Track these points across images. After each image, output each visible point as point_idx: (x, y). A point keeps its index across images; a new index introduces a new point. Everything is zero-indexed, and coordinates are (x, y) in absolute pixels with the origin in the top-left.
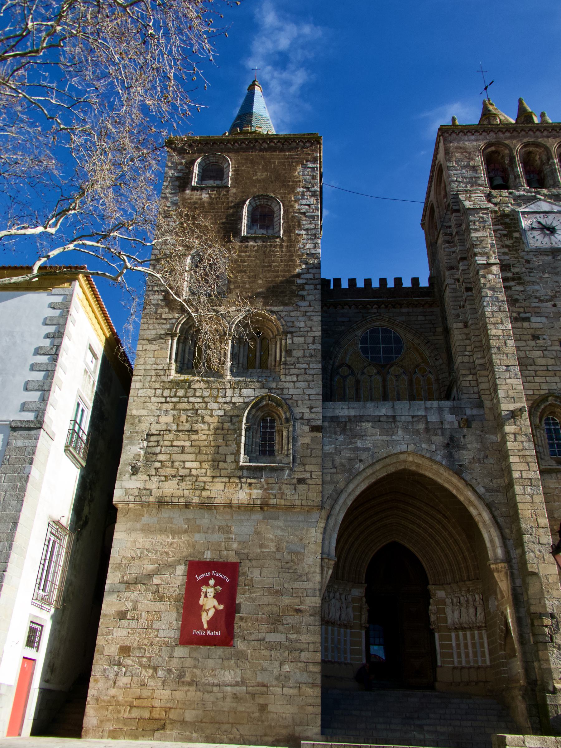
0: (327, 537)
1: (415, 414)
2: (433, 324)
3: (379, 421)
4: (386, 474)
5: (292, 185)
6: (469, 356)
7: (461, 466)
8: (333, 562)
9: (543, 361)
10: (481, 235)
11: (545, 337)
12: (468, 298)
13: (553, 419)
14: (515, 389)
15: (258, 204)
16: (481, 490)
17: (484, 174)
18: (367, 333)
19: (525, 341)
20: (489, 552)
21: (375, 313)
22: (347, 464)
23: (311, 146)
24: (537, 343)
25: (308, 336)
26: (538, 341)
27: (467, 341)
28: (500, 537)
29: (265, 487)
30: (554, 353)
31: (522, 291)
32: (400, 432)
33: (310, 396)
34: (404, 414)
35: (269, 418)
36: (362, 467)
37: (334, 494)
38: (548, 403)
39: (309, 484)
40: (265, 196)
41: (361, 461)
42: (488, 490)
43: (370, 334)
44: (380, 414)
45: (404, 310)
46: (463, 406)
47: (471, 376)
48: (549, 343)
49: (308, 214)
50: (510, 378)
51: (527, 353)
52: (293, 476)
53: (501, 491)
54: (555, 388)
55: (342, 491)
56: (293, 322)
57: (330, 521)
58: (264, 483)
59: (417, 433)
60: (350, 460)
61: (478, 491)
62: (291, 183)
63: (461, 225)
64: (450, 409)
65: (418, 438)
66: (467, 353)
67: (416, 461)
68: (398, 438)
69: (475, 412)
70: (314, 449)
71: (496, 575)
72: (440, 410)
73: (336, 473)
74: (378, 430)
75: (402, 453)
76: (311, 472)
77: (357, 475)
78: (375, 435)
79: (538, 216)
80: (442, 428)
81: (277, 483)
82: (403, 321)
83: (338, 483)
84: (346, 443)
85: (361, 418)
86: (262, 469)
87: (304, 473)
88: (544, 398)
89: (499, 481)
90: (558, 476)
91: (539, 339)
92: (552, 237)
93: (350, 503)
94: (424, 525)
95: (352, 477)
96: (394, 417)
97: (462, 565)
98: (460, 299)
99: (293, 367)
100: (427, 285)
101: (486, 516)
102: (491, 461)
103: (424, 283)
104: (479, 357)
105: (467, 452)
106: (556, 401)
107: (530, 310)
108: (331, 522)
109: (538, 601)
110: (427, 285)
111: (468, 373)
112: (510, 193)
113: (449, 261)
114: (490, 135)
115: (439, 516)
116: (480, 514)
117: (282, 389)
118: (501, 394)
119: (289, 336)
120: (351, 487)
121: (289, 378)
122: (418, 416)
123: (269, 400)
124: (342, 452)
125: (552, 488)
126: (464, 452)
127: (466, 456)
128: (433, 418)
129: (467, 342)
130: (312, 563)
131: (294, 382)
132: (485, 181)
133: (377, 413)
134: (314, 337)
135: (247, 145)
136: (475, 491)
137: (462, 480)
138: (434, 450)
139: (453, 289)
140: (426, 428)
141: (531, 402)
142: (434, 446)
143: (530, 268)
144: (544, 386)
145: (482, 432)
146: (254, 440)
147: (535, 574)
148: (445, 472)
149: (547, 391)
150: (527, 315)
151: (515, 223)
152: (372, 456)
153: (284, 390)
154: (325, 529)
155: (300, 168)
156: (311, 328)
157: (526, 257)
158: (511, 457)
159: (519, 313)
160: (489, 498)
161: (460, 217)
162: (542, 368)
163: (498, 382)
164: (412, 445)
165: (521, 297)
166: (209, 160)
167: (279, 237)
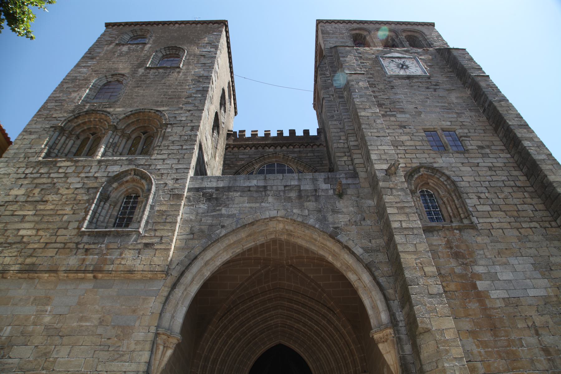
0: (170, 308)
1: (287, 184)
2: (321, 159)
3: (249, 191)
4: (253, 243)
6: (344, 143)
7: (336, 228)
8: (175, 341)
9: (412, 143)
11: (411, 127)
12: (341, 102)
13: (427, 191)
14: (387, 153)
15: (168, 53)
16: (359, 251)
18: (264, 167)
19: (394, 129)
20: (372, 321)
21: (271, 152)
22: (206, 231)
24: (404, 131)
25: (187, 126)
26: (405, 130)
27: (342, 133)
28: (383, 299)
29: (104, 252)
30: (421, 138)
31: (386, 99)
32: (270, 199)
33: (178, 170)
34: (276, 184)
35: (134, 195)
36: (223, 234)
37: (187, 260)
38: (420, 174)
39: (156, 249)
40: (174, 47)
41: (223, 227)
42: (366, 250)
43: (267, 167)
44: (250, 185)
45: (296, 150)
46: (338, 176)
47: (346, 157)
48: (415, 131)
50: (381, 145)
51: (397, 137)
52: (139, 241)
53: (381, 250)
54: (426, 161)
55: (196, 258)
56: (175, 117)
57: (176, 290)
58: (104, 248)
59: (289, 199)
60: (211, 226)
61: (356, 252)
64: (325, 179)
65: (290, 204)
66: (341, 141)
67: (287, 227)
68: (268, 205)
69: (350, 181)
70: (170, 215)
71: (381, 346)
72: (314, 180)
73: (193, 239)
74: (246, 198)
75: (271, 219)
76: (161, 237)
77: (217, 240)
78: (244, 202)
80: (316, 195)
81: (119, 248)
82: (296, 157)
83: (193, 248)
84: (210, 211)
85: (229, 189)
86: (107, 234)
87: (153, 238)
88: (416, 170)
89: (378, 241)
90: (440, 233)
91: (406, 128)
92: (406, 70)
93: (207, 274)
94: (310, 322)
95: (210, 243)
96: (265, 187)
97: (349, 361)
98: (335, 106)
99: (166, 148)
100: (316, 134)
101: (366, 278)
102: (369, 222)
103: (313, 132)
104: (353, 140)
105: (343, 216)
106: (428, 172)
107: (395, 110)
108: (178, 292)
109: (435, 364)
110: (316, 134)
111: (344, 155)
115: (324, 311)
116: (359, 279)
117: (150, 165)
118: (373, 157)
119: (169, 126)
120: (209, 255)
121: (159, 157)
122: (291, 185)
123: (135, 174)
124: (203, 219)
125: (435, 245)
126: (340, 216)
127: (342, 219)
128: (307, 186)
129: (342, 134)
130: (141, 338)
131: (164, 160)
133: (247, 184)
134: (194, 126)
136: (353, 253)
137: (338, 244)
138: (307, 214)
139: (329, 101)
140: (298, 196)
141: (405, 172)
142: (307, 211)
143: (392, 86)
144: (414, 161)
145: (358, 197)
146: (110, 211)
147: (428, 331)
148: (319, 236)
149: (419, 164)
150: (393, 113)
152: (237, 222)
153: (152, 166)
154: (167, 298)
156: (192, 121)
157: (387, 80)
158: (388, 208)
159: (386, 112)
160: (367, 258)
162: (411, 148)
163: (370, 148)
164: (283, 211)
165: (387, 102)
167: (179, 67)
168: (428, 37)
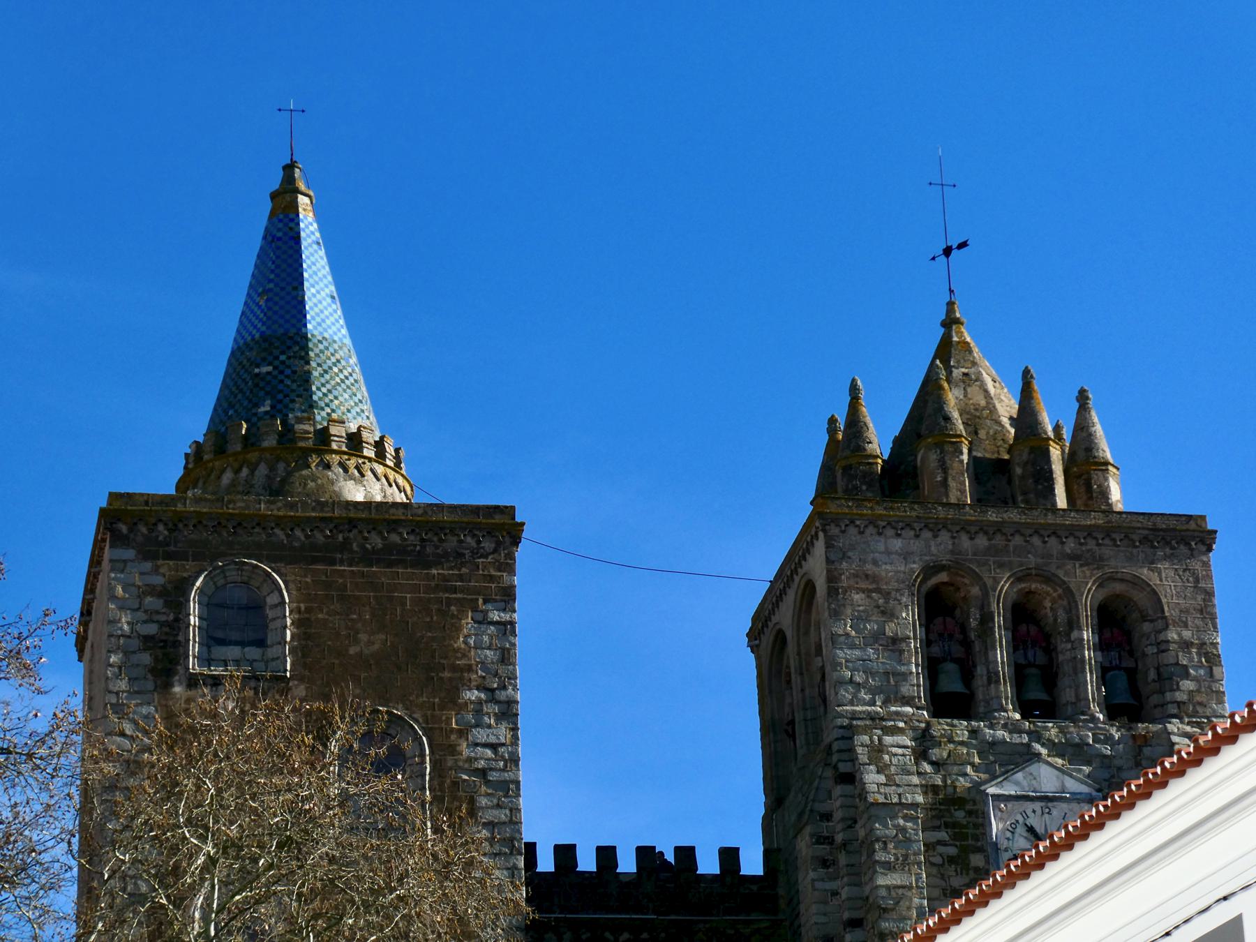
5: (450, 679)
10: (899, 883)
17: (917, 665)
23: (495, 551)
49: (493, 776)
62: (447, 674)
63: (855, 822)
79: (1029, 807)
103: (752, 864)
112: (974, 733)
113: (822, 919)
114: (939, 539)
132: (918, 686)
135: (326, 537)
151: (976, 826)
155: (468, 623)
161: (852, 797)
166: (225, 577)
168: (1172, 635)
